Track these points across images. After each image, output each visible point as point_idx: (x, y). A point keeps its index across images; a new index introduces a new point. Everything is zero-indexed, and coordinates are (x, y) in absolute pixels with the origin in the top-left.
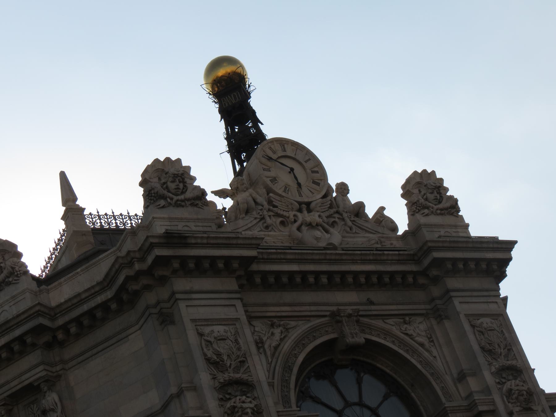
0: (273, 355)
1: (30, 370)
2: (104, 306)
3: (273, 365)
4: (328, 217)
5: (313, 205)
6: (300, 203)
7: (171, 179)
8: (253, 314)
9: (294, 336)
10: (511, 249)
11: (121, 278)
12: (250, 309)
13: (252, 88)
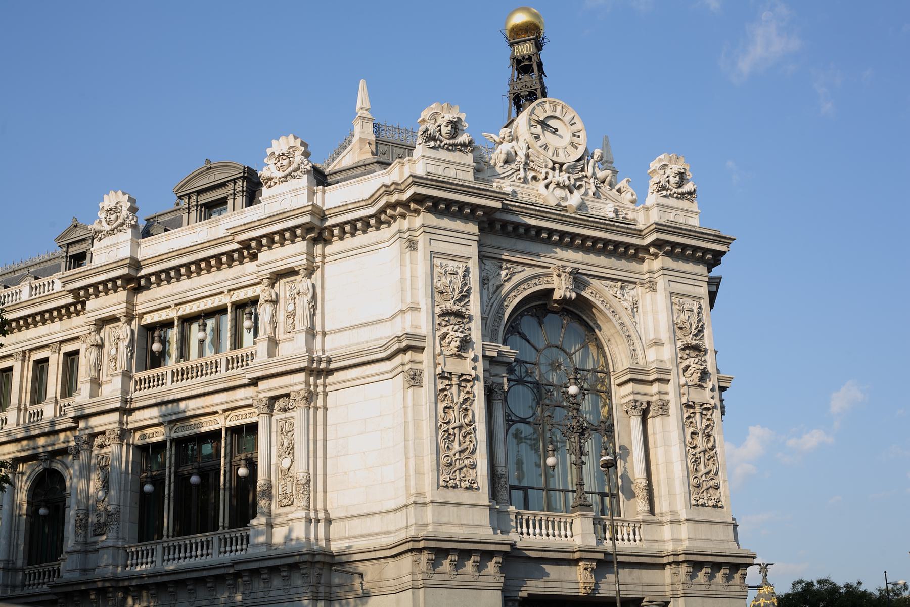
0: (495, 292)
1: (295, 256)
2: (366, 221)
3: (492, 301)
4: (576, 180)
5: (564, 167)
6: (554, 163)
7: (445, 124)
8: (487, 254)
9: (516, 279)
10: (728, 244)
11: (382, 202)
12: (485, 249)
13: (545, 41)
